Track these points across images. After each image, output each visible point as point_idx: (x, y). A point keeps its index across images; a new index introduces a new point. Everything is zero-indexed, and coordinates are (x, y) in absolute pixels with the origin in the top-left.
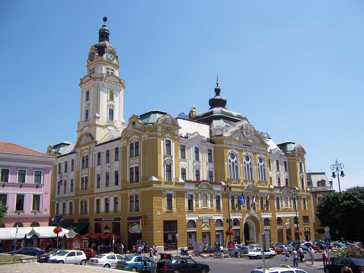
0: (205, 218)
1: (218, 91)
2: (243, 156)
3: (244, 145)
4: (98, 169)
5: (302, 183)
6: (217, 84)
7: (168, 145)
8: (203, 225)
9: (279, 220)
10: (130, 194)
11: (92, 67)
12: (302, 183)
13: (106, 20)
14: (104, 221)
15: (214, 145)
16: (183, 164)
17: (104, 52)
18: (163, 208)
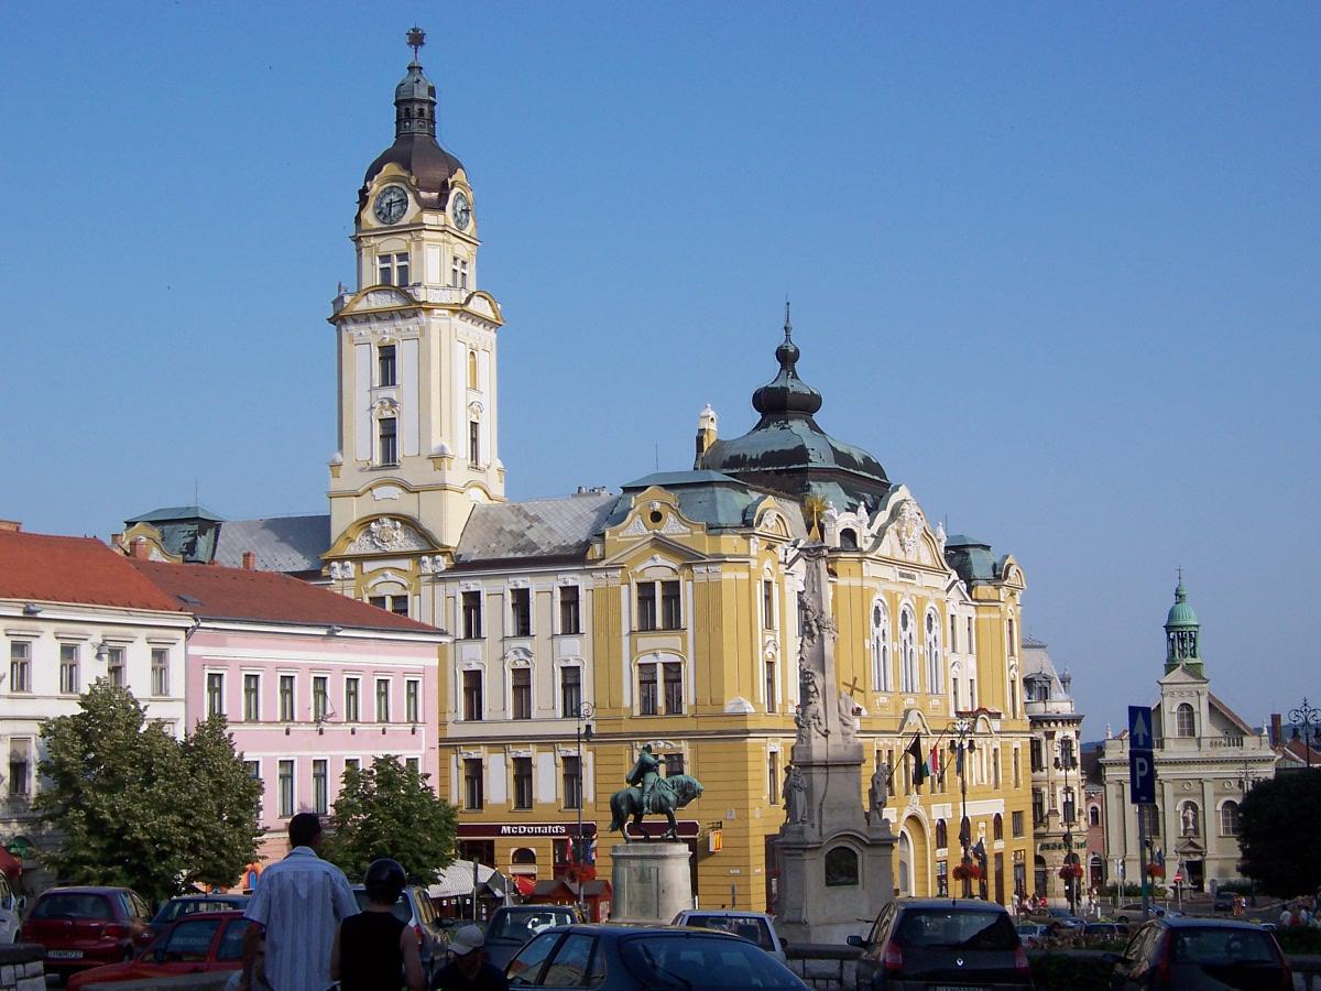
1: (786, 358)
13: (422, 44)
14: (507, 834)
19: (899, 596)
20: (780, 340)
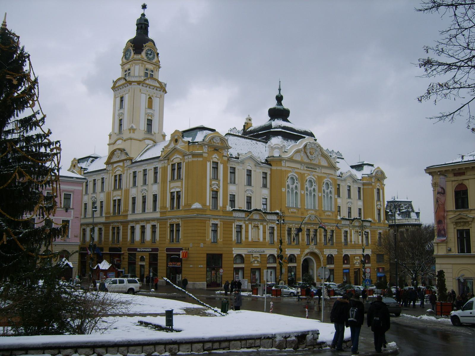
0: (255, 252)
1: (279, 99)
2: (305, 181)
3: (307, 167)
4: (133, 192)
5: (379, 214)
6: (280, 90)
7: (215, 168)
8: (253, 259)
9: (346, 259)
10: (170, 222)
11: (127, 67)
12: (379, 214)
13: (146, 8)
15: (271, 167)
16: (232, 189)
17: (143, 48)
18: (207, 240)
19: (306, 175)
20: (277, 93)
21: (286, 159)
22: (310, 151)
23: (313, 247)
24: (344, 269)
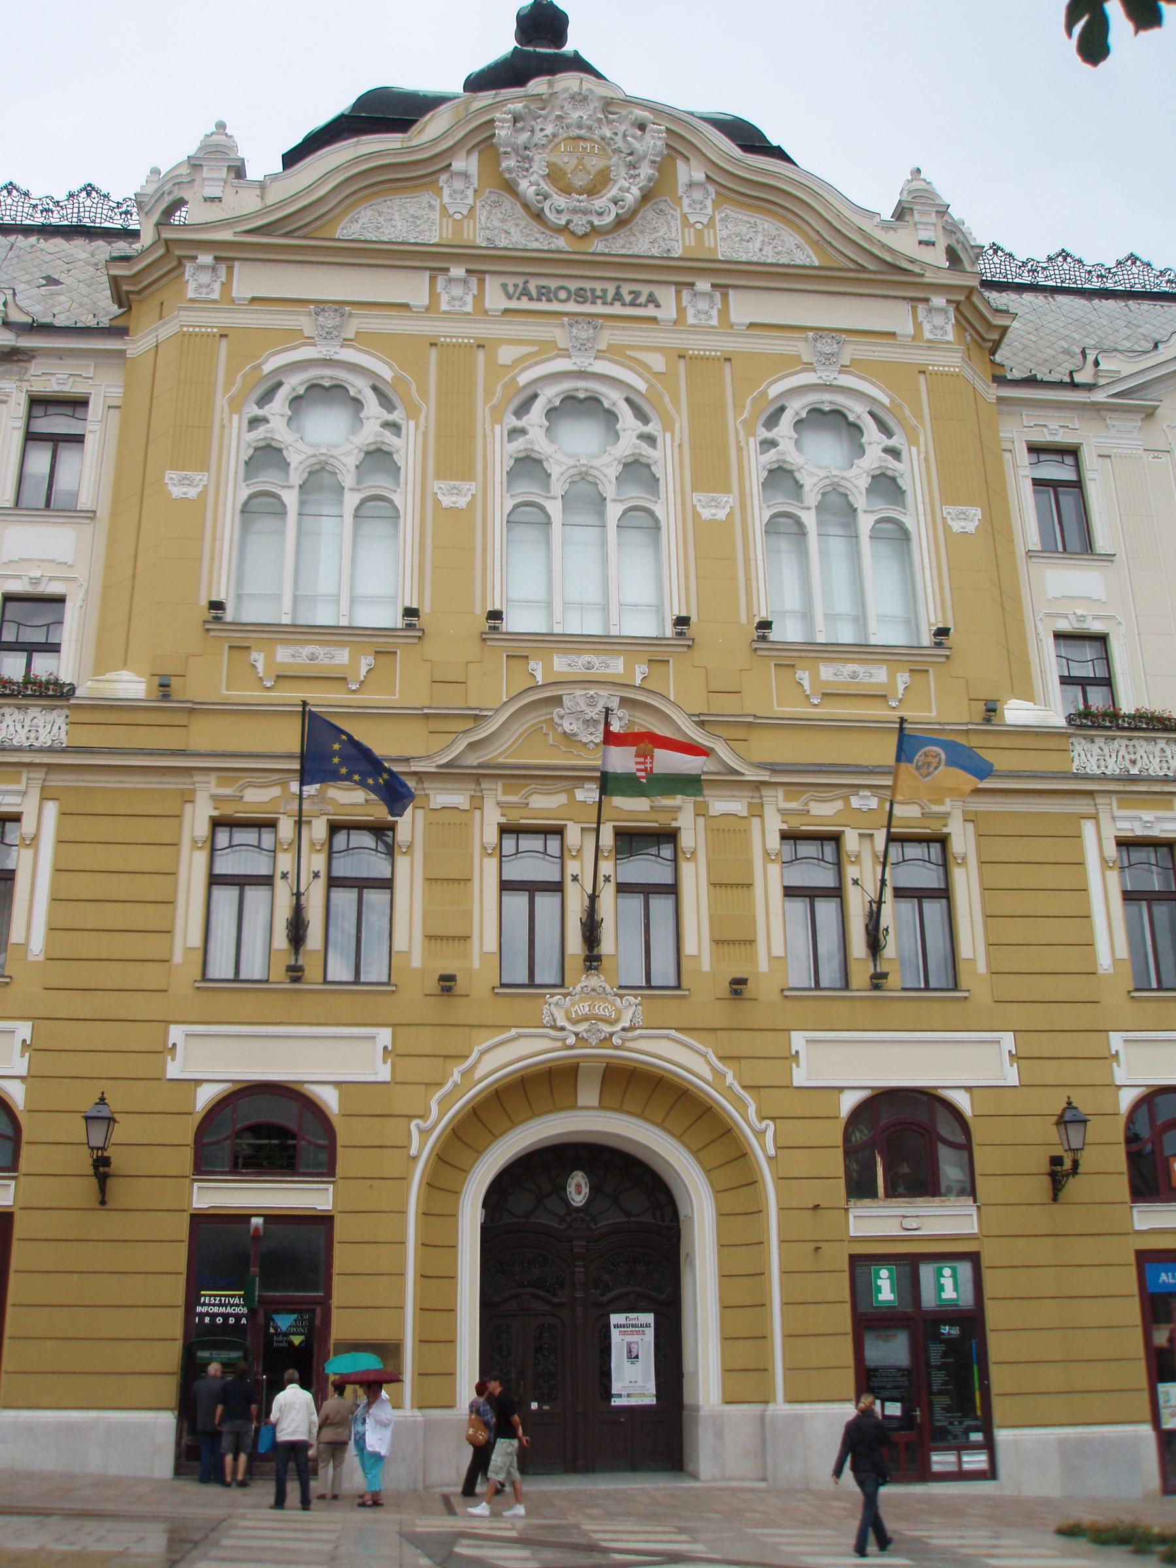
21: (226, 235)
22: (550, 165)
23: (601, 1009)
24: (1145, 1258)
